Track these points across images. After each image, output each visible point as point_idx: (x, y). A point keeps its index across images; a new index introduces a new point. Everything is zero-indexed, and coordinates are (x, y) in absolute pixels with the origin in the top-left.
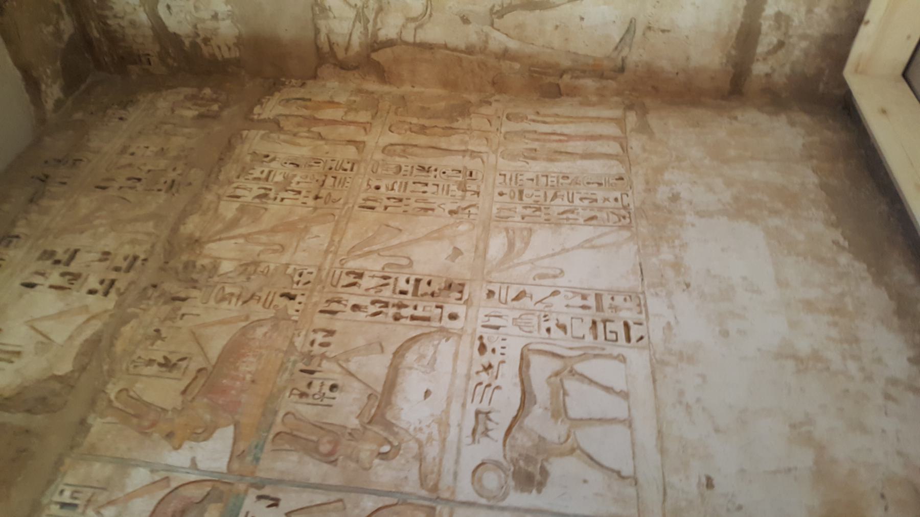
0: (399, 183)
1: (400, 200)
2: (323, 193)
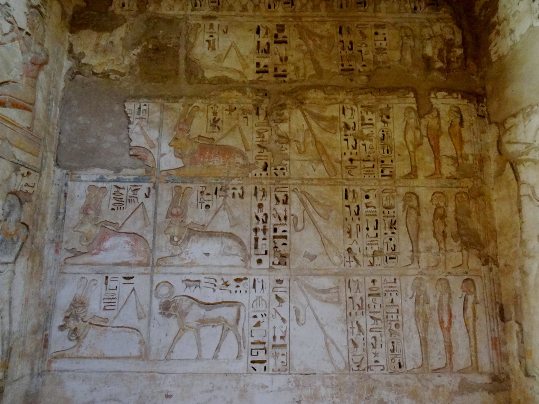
0: (374, 210)
1: (357, 214)
2: (355, 163)
